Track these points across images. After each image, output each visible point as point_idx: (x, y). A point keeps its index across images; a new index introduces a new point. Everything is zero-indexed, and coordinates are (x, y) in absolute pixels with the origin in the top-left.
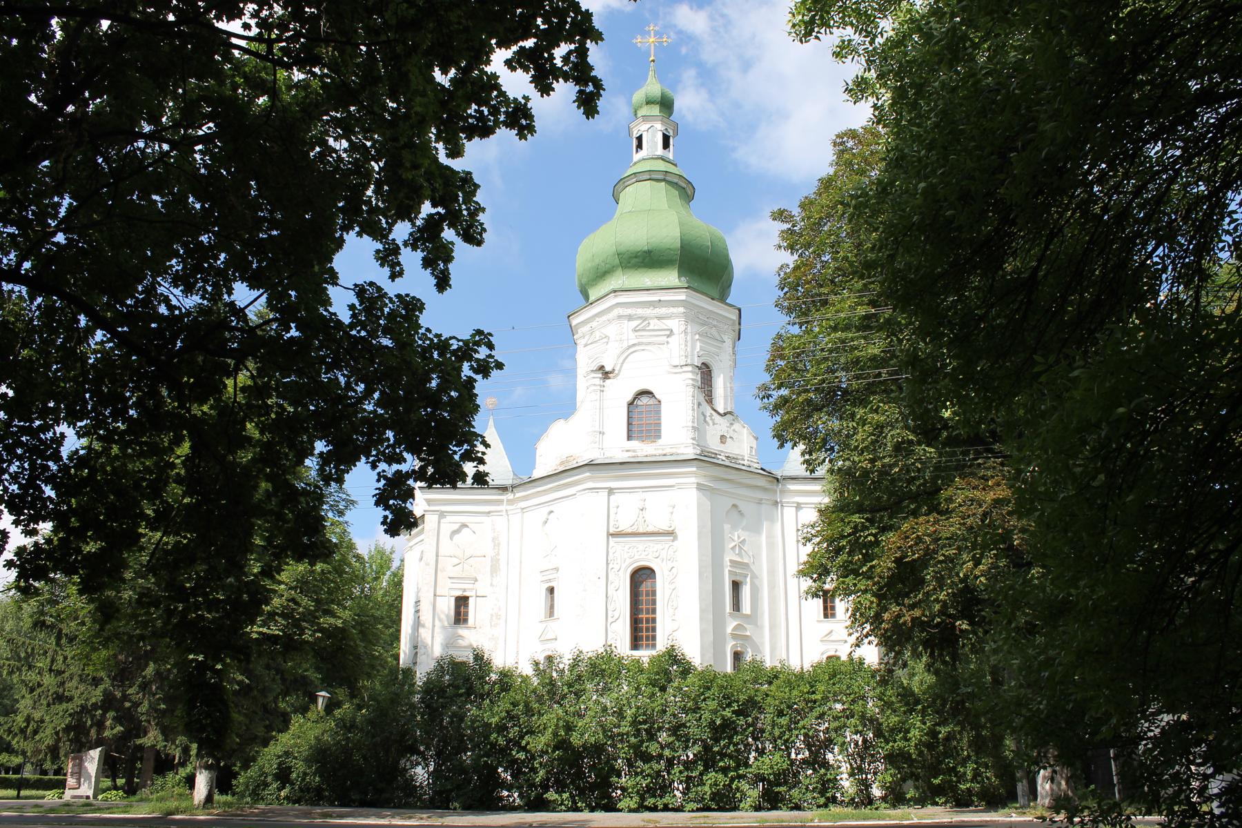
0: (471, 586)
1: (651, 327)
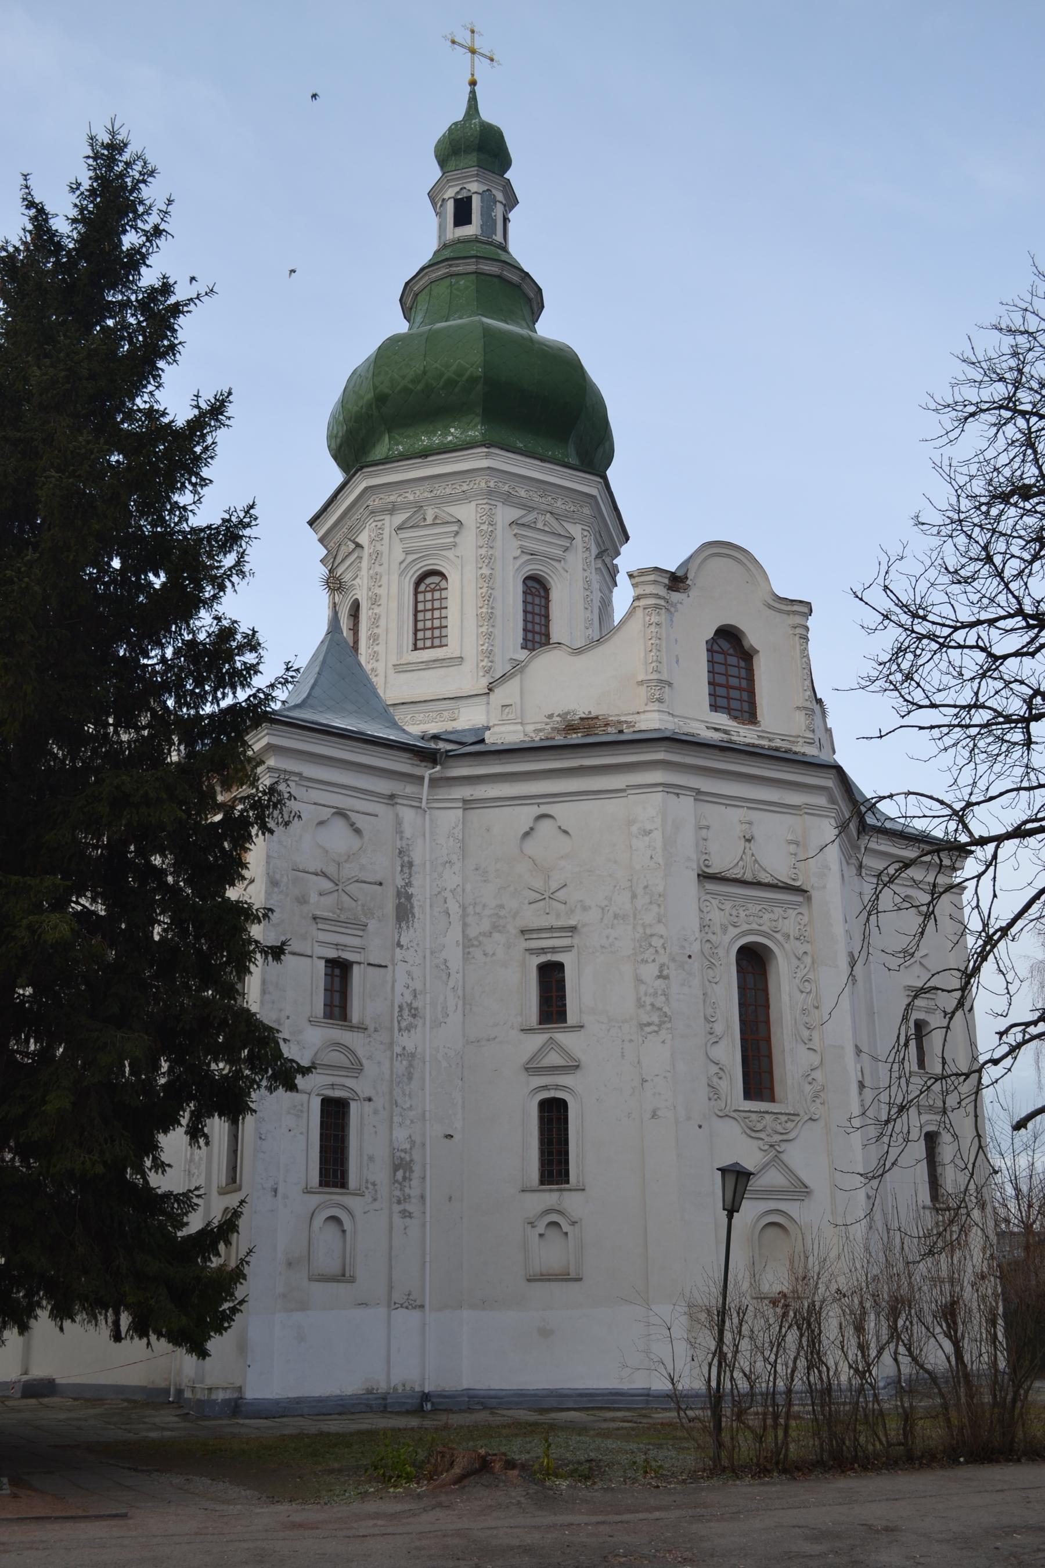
1: (540, 526)
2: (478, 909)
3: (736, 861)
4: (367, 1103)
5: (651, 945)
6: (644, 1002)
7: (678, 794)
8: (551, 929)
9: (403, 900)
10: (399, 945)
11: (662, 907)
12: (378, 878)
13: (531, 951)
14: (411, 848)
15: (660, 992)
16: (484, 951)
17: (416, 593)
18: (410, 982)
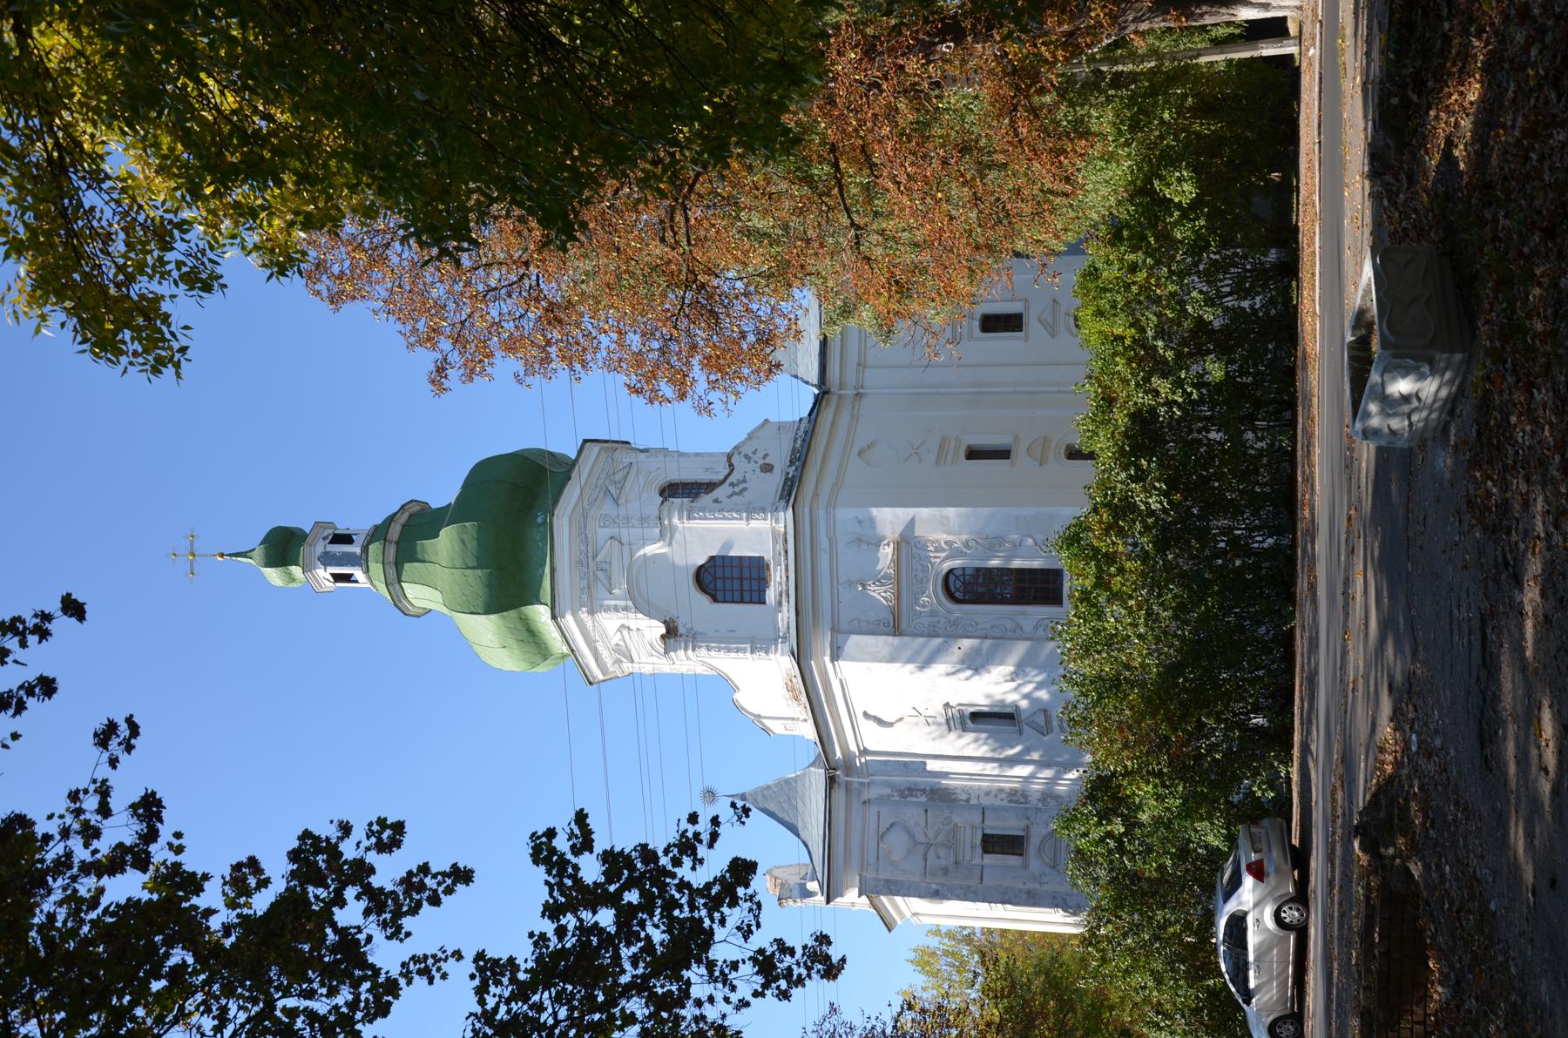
7: (838, 648)
10: (968, 800)
12: (922, 812)
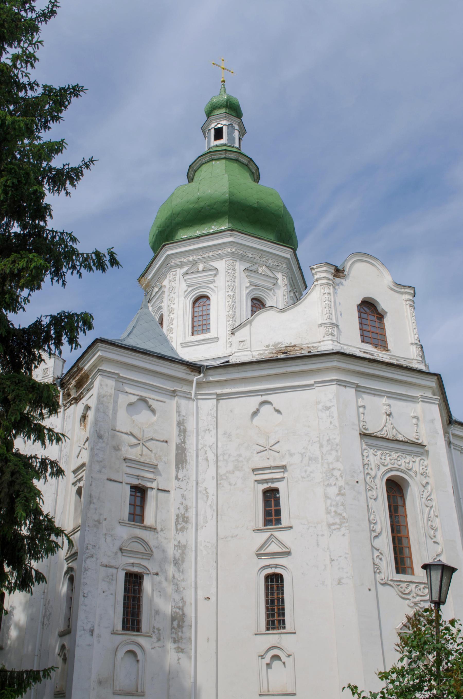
0: (151, 476)
2: (226, 457)
3: (382, 427)
4: (155, 576)
5: (333, 475)
6: (330, 510)
7: (345, 386)
8: (270, 468)
9: (180, 451)
11: (339, 452)
12: (165, 439)
13: (258, 482)
14: (185, 421)
15: (340, 504)
16: (229, 482)
17: (193, 307)
18: (184, 501)
